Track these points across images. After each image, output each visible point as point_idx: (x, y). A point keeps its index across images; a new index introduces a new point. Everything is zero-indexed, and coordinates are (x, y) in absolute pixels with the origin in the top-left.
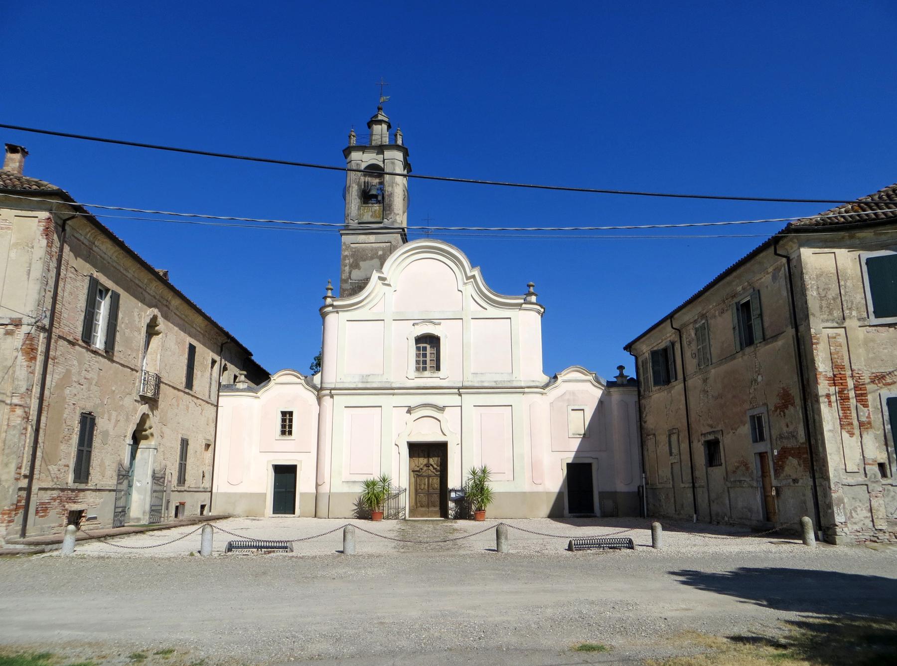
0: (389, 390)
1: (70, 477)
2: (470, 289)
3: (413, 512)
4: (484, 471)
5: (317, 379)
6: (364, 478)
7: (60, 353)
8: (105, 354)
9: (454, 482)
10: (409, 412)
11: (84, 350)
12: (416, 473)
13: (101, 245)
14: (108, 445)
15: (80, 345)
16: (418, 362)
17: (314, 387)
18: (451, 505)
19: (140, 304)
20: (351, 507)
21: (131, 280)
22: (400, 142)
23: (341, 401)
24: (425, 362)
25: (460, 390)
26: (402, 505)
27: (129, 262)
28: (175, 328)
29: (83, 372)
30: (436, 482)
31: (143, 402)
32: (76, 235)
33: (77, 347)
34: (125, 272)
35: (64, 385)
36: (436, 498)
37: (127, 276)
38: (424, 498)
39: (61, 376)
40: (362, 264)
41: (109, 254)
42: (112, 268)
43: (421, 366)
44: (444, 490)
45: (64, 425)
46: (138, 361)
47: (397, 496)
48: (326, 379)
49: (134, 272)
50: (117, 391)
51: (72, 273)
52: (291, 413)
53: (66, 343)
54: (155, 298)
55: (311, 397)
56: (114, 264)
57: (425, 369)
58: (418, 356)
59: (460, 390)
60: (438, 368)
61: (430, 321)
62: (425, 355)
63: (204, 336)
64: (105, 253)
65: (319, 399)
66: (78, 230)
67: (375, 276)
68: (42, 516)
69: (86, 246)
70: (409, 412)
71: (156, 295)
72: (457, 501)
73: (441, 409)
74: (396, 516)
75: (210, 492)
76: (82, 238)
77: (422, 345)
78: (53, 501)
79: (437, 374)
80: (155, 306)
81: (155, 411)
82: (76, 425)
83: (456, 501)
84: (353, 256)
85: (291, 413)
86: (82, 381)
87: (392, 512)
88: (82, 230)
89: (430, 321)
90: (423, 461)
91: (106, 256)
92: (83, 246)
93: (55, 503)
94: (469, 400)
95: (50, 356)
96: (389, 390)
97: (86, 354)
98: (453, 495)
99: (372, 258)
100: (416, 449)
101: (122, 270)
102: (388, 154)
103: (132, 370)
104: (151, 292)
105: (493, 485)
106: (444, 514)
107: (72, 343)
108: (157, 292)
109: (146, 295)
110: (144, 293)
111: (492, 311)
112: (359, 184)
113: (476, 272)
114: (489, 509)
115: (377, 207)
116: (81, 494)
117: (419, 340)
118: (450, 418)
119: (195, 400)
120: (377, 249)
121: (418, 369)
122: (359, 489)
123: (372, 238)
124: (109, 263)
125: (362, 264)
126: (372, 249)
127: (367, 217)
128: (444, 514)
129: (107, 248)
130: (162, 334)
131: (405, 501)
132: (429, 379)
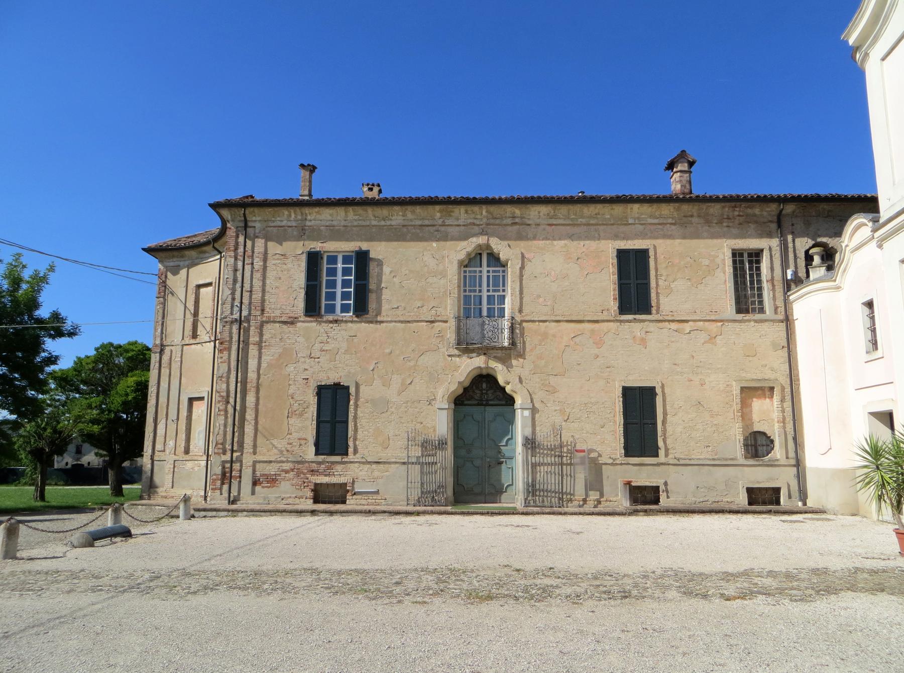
1: (310, 452)
7: (270, 336)
8: (356, 319)
11: (314, 324)
13: (318, 216)
14: (389, 413)
15: (303, 322)
19: (434, 244)
21: (404, 226)
27: (384, 211)
28: (555, 243)
29: (316, 345)
31: (474, 355)
32: (273, 224)
33: (299, 324)
34: (383, 223)
35: (282, 363)
37: (391, 225)
39: (277, 356)
41: (339, 218)
42: (354, 229)
45: (291, 400)
46: (446, 308)
49: (403, 216)
50: (398, 352)
51: (278, 259)
53: (278, 325)
54: (474, 224)
56: (355, 223)
63: (683, 225)
64: (332, 221)
66: (273, 219)
68: (266, 487)
69: (295, 227)
71: (475, 221)
75: (794, 466)
76: (284, 223)
78: (284, 473)
80: (483, 233)
81: (514, 362)
82: (312, 398)
86: (316, 353)
88: (279, 217)
91: (335, 223)
92: (290, 229)
93: (287, 475)
95: (250, 342)
97: (318, 327)
101: (374, 223)
103: (432, 322)
104: (461, 222)
107: (292, 322)
108: (479, 217)
109: (450, 229)
110: (443, 229)
116: (339, 467)
119: (674, 326)
124: (344, 226)
129: (331, 215)
130: (510, 261)
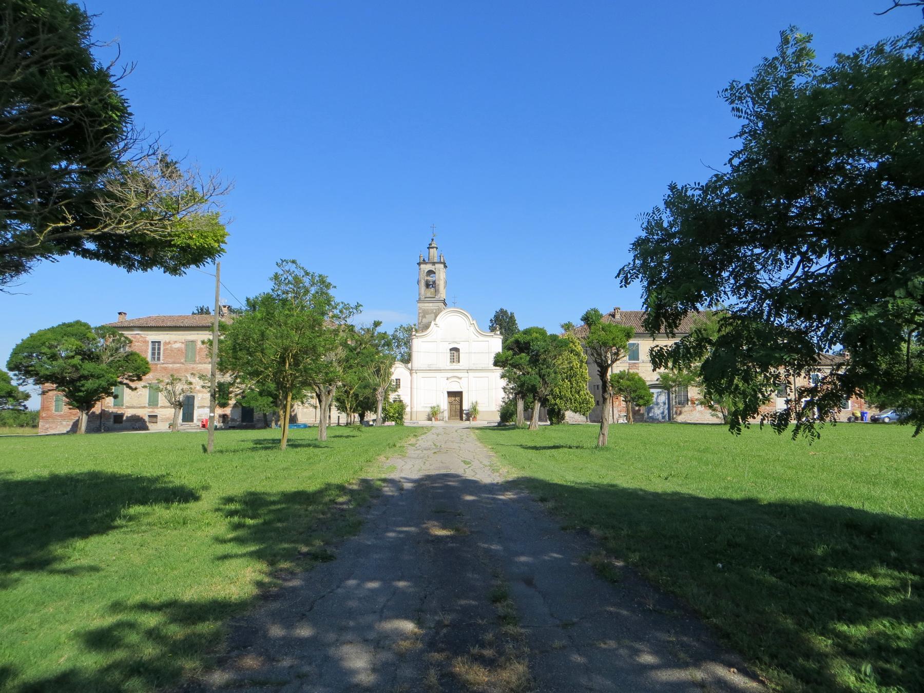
0: (439, 370)
2: (472, 329)
3: (449, 419)
4: (476, 403)
5: (409, 365)
6: (430, 405)
9: (466, 406)
10: (447, 379)
12: (450, 403)
16: (451, 359)
17: (409, 369)
18: (464, 416)
20: (426, 417)
22: (442, 261)
23: (420, 375)
24: (454, 359)
25: (468, 371)
26: (445, 416)
30: (458, 407)
36: (458, 413)
38: (454, 414)
40: (427, 316)
43: (452, 361)
44: (461, 410)
47: (443, 412)
48: (413, 366)
52: (399, 380)
55: (408, 373)
57: (454, 362)
58: (451, 356)
59: (468, 371)
60: (459, 362)
61: (456, 342)
62: (453, 356)
65: (411, 374)
67: (433, 323)
70: (447, 379)
72: (467, 414)
73: (460, 378)
74: (443, 420)
77: (452, 352)
79: (459, 364)
83: (467, 414)
84: (423, 312)
85: (399, 380)
87: (441, 418)
89: (456, 342)
90: (453, 399)
94: (471, 374)
96: (439, 370)
98: (465, 412)
99: (431, 313)
100: (450, 394)
102: (437, 266)
105: (479, 408)
106: (461, 419)
111: (481, 338)
112: (424, 280)
113: (474, 322)
114: (478, 417)
115: (432, 290)
117: (451, 350)
118: (464, 382)
120: (433, 309)
121: (451, 362)
122: (429, 410)
123: (431, 304)
125: (427, 316)
126: (431, 309)
127: (429, 295)
128: (461, 419)
131: (446, 414)
132: (455, 366)
